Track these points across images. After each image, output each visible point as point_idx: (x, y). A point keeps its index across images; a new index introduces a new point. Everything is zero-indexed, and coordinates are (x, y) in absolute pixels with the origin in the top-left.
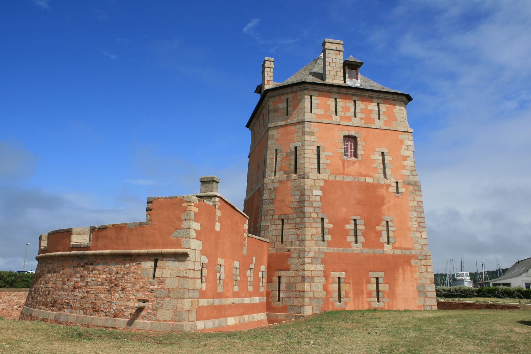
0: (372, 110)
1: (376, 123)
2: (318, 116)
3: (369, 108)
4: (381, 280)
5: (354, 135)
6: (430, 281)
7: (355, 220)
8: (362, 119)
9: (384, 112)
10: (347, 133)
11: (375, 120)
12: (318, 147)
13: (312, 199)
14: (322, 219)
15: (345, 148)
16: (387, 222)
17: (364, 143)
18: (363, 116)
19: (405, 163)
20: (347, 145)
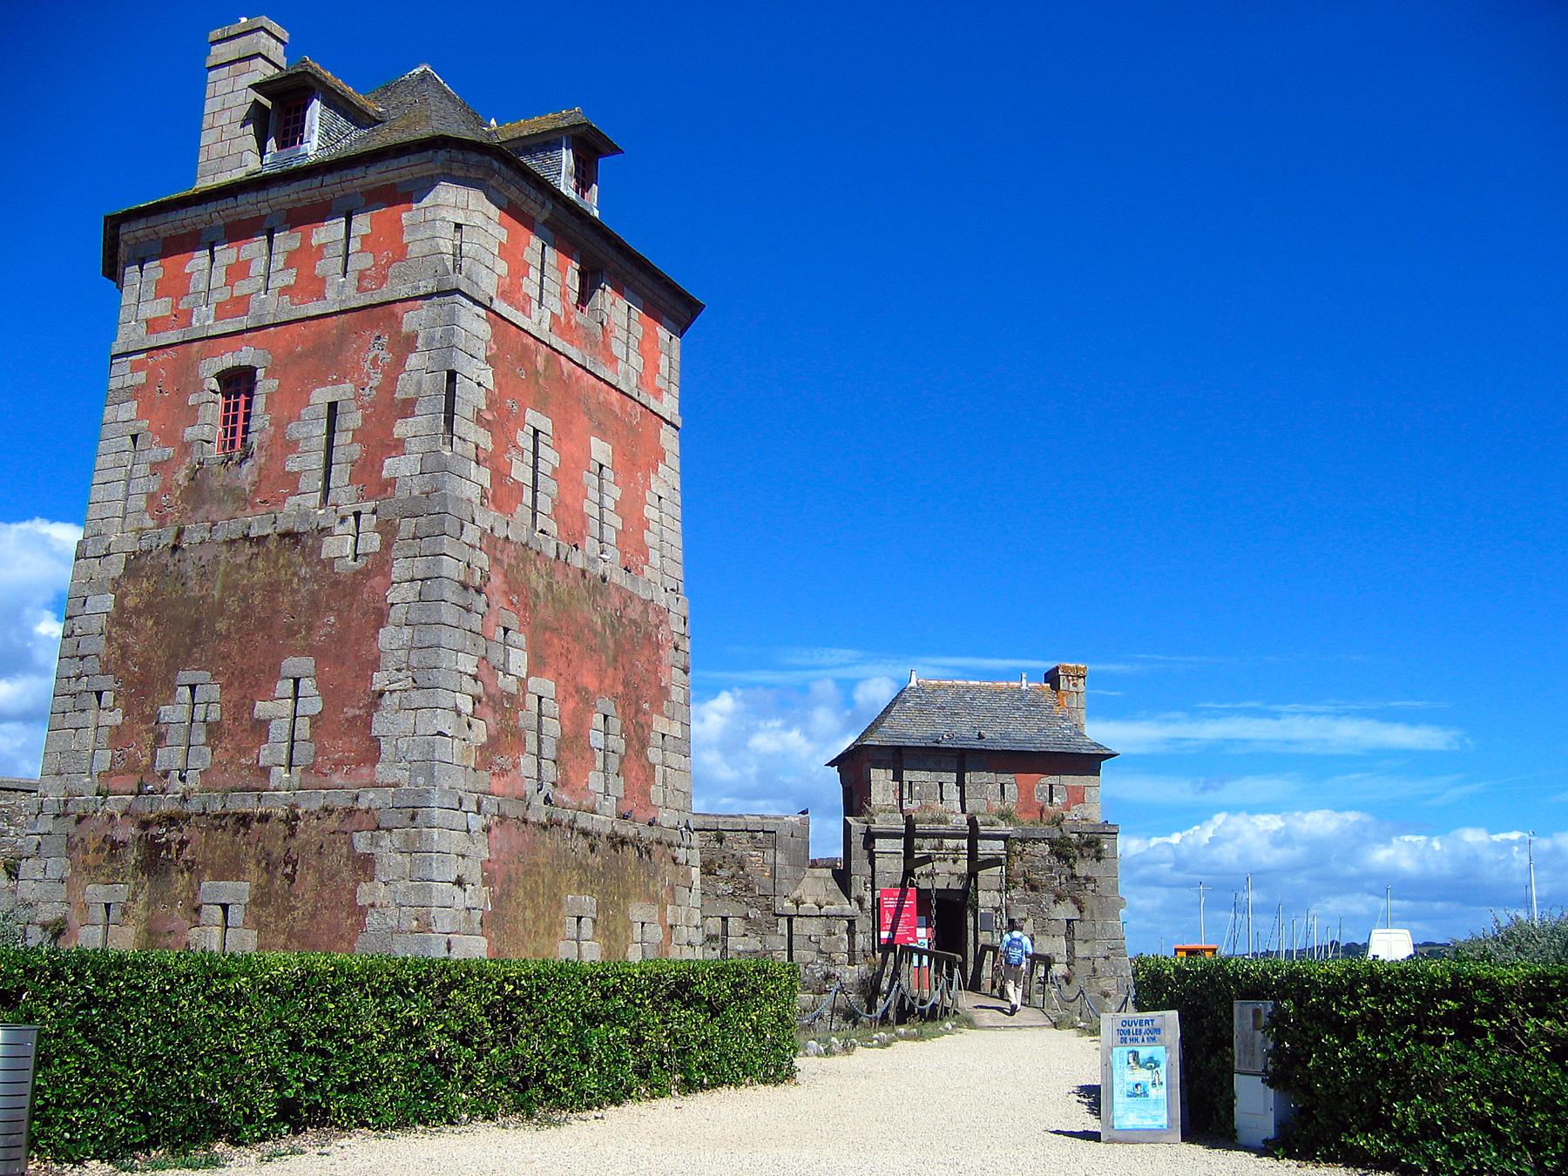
0: (324, 245)
1: (330, 294)
2: (153, 325)
3: (314, 242)
4: (236, 914)
5: (247, 364)
6: (417, 919)
7: (193, 688)
8: (284, 291)
9: (365, 238)
10: (228, 361)
11: (329, 280)
12: (134, 438)
13: (81, 628)
14: (99, 694)
15: (226, 422)
16: (297, 681)
17: (273, 384)
18: (289, 278)
19: (401, 429)
20: (236, 406)
